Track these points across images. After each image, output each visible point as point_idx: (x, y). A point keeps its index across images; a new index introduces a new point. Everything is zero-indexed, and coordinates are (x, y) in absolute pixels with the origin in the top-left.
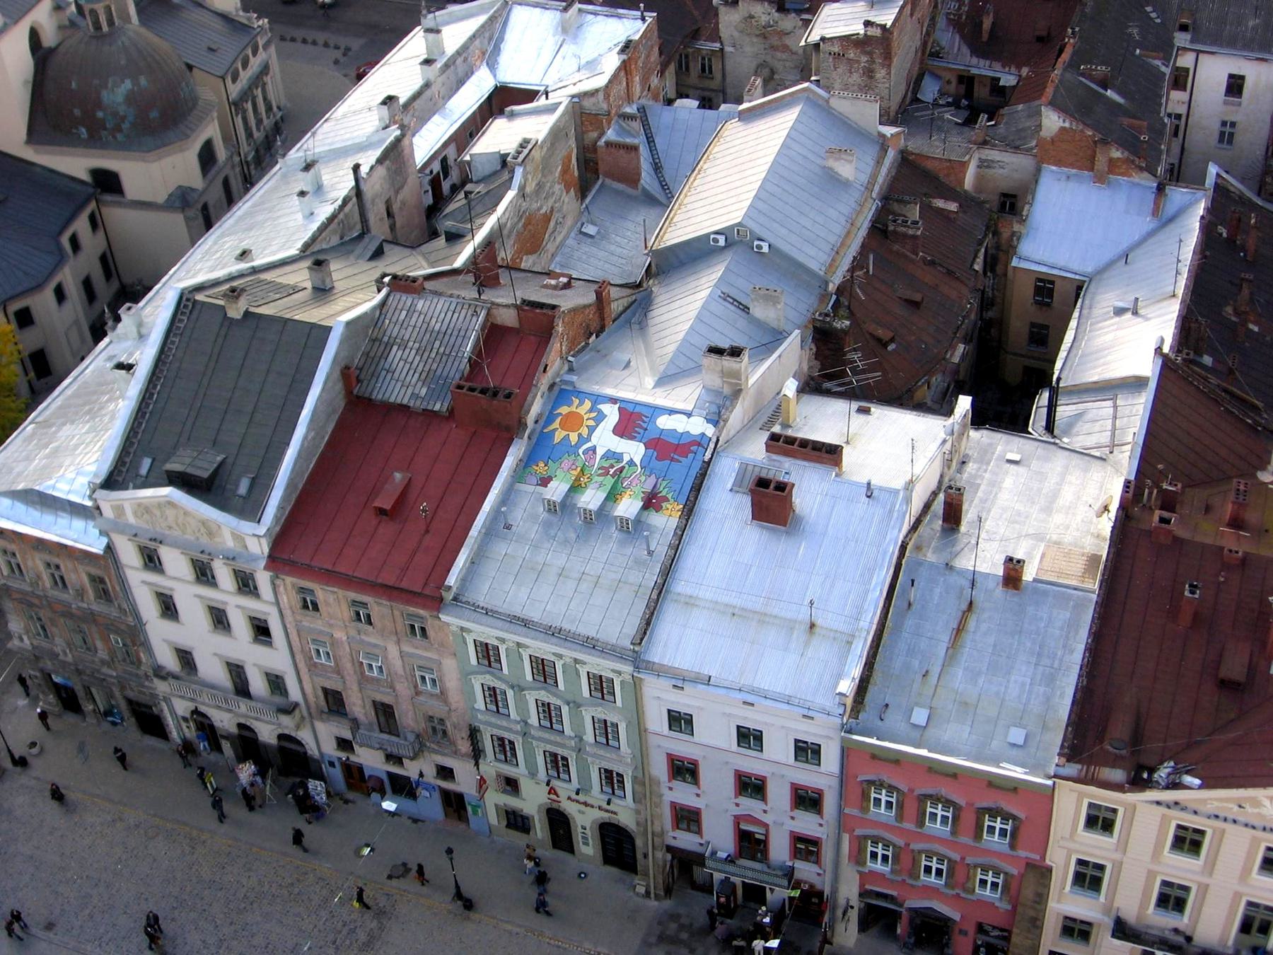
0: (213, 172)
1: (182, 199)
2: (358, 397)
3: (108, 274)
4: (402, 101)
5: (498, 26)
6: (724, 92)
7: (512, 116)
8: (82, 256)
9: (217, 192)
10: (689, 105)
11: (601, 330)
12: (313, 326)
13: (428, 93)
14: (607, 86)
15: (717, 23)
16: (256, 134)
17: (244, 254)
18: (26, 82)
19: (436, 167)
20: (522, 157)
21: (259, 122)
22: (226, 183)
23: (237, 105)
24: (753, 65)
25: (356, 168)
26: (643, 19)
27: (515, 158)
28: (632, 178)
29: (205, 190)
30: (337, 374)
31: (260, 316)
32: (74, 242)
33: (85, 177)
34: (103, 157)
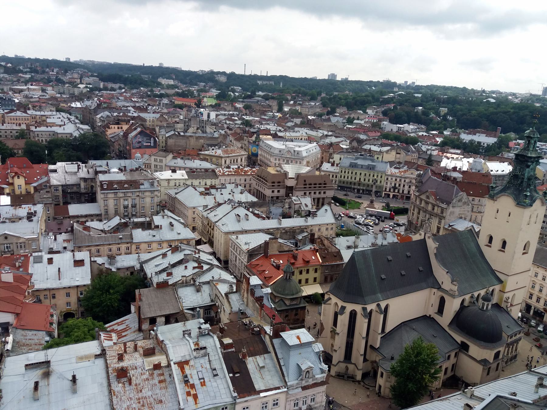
0: (496, 360)
1: (484, 362)
3: (452, 370)
9: (495, 364)
16: (509, 355)
17: (514, 394)
18: (456, 311)
21: (512, 352)
23: (508, 345)
29: (492, 363)
32: (449, 357)
33: (459, 342)
34: (467, 340)
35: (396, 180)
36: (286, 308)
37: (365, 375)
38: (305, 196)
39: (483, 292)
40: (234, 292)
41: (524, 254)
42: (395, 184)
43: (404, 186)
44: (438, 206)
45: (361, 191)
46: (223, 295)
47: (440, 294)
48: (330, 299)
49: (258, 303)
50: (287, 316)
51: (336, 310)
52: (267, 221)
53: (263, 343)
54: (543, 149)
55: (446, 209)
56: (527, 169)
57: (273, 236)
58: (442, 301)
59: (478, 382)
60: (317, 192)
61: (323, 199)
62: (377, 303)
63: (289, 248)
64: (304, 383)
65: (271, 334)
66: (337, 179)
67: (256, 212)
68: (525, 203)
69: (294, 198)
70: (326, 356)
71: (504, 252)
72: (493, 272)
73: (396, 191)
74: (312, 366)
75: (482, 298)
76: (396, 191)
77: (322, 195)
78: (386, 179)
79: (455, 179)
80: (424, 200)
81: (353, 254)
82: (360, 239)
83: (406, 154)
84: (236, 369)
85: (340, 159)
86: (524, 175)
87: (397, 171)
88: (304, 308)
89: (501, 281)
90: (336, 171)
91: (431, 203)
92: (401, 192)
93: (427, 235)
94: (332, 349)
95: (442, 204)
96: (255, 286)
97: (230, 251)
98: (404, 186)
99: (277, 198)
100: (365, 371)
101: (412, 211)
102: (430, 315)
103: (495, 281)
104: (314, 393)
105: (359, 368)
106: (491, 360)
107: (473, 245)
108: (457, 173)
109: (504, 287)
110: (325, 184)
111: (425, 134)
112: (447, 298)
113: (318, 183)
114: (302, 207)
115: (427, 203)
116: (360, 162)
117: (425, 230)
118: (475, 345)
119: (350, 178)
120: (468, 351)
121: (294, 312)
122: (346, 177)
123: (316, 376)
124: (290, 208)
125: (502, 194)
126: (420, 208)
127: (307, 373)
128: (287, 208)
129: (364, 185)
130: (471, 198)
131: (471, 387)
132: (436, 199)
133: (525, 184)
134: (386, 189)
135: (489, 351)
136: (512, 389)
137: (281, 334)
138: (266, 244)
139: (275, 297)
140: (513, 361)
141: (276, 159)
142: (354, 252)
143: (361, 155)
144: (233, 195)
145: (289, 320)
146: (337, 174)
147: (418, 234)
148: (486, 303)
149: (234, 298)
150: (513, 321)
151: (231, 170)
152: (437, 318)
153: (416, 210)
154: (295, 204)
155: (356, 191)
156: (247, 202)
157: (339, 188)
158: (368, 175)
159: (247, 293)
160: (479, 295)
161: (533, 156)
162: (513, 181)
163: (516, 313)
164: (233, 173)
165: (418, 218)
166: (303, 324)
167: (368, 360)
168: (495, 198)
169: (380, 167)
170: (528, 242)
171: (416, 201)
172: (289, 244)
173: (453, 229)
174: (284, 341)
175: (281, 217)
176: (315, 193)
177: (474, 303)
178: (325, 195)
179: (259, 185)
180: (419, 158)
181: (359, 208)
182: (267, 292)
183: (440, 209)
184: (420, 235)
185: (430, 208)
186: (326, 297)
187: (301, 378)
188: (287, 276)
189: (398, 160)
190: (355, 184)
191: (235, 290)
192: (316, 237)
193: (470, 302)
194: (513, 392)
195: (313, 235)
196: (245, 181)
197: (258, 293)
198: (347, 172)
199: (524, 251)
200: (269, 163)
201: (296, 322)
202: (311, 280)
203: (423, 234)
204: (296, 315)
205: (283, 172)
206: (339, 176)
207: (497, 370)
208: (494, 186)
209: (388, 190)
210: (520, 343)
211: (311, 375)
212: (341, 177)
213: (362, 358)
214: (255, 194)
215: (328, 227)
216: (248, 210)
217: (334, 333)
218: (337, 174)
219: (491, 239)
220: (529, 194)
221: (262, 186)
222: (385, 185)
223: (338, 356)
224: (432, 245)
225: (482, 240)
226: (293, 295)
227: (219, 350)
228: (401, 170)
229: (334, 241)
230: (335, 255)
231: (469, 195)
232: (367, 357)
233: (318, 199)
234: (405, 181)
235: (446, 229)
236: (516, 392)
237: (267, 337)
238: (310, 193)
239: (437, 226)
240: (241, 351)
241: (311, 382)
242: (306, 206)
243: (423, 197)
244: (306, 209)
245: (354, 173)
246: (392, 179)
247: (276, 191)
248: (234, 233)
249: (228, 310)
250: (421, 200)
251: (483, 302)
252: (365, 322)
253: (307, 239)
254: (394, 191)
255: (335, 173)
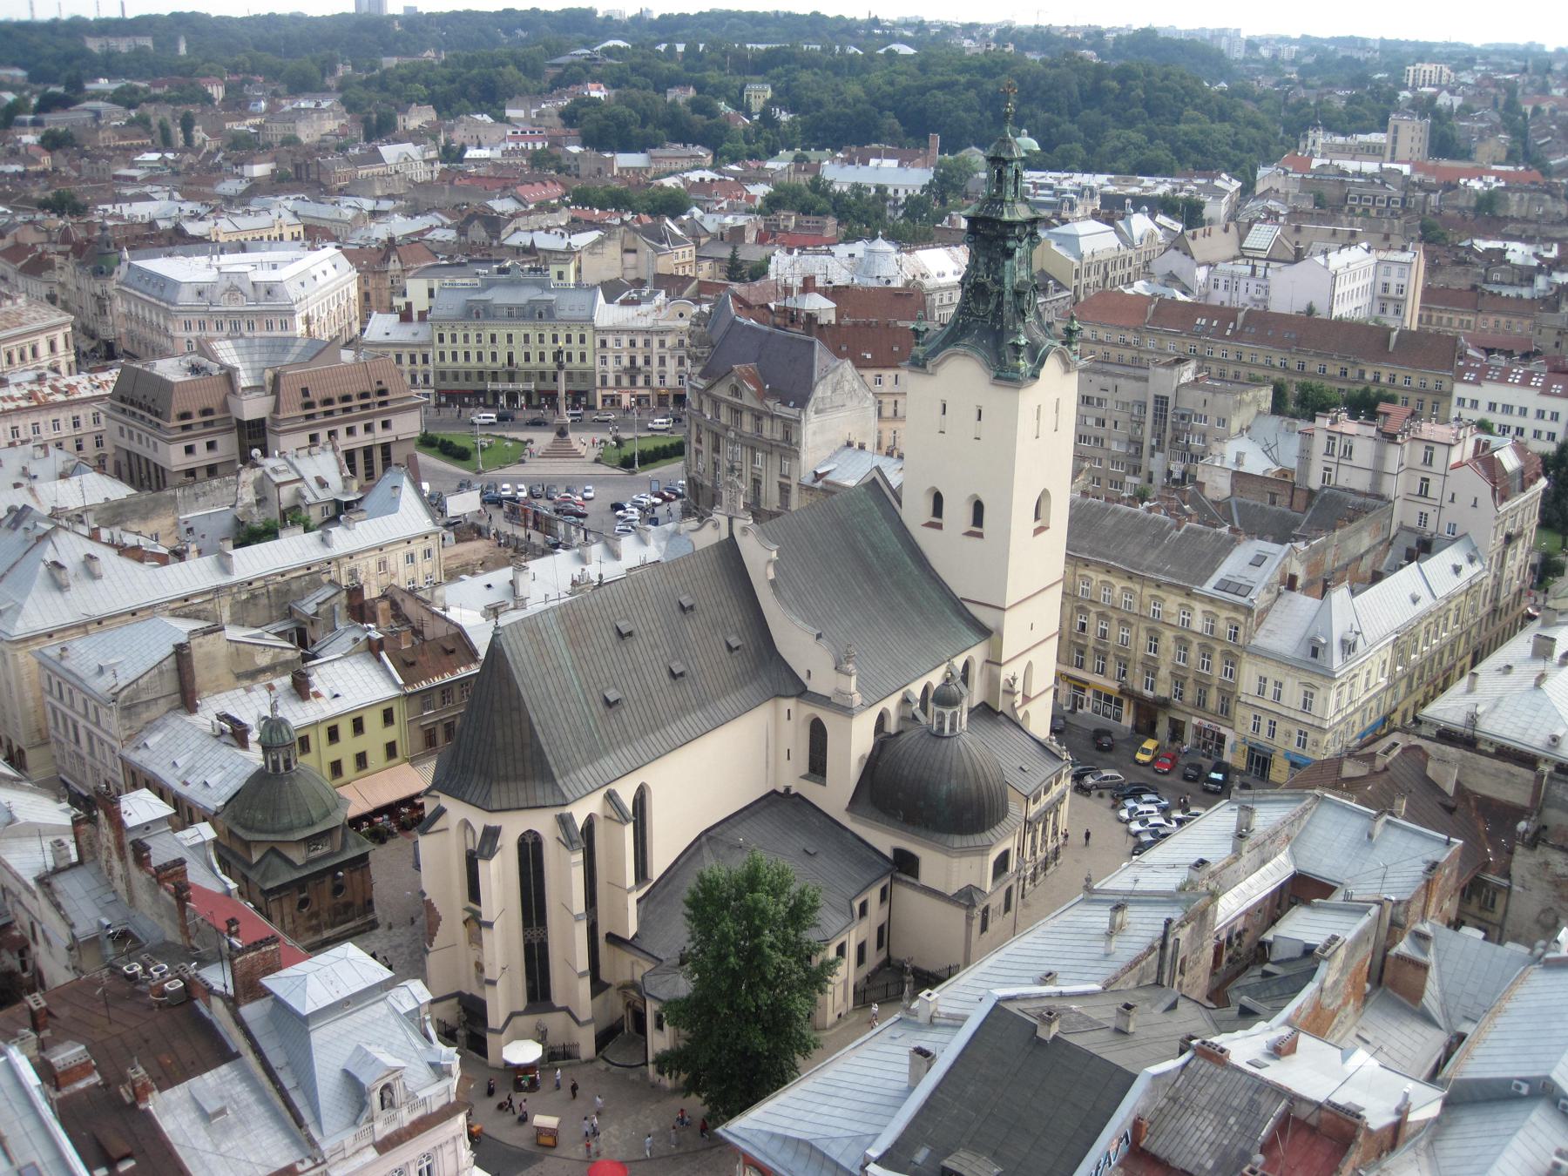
0: (1001, 880)
1: (967, 898)
2: (1142, 1150)
3: (880, 945)
4: (1214, 867)
5: (1307, 817)
6: (1501, 927)
7: (1319, 907)
8: (865, 923)
10: (1473, 934)
11: (1393, 1147)
12: (1118, 1069)
13: (1235, 866)
14: (1409, 902)
15: (1509, 862)
16: (1038, 853)
17: (1049, 977)
19: (1223, 937)
20: (1329, 951)
21: (1045, 842)
22: (1009, 892)
24: (1538, 909)
25: (1169, 922)
26: (1448, 843)
27: (1323, 951)
28: (1416, 994)
30: (1129, 1122)
31: (1068, 1044)
32: (863, 908)
33: (888, 853)
34: (911, 841)
35: (633, 343)
36: (297, 875)
37: (604, 1039)
38: (314, 450)
39: (936, 678)
40: (72, 866)
41: (1038, 531)
42: (633, 360)
43: (662, 361)
44: (772, 417)
45: (522, 400)
46: (32, 883)
47: (808, 710)
48: (440, 812)
49: (166, 889)
50: (304, 903)
51: (470, 846)
52: (175, 568)
53: (207, 1028)
54: (1064, 192)
55: (799, 422)
56: (1008, 263)
57: (206, 619)
58: (818, 733)
59: (960, 961)
60: (359, 427)
61: (386, 447)
62: (604, 791)
63: (275, 656)
64: (382, 1129)
65: (231, 991)
66: (430, 367)
67: (130, 540)
68: (1017, 370)
69: (269, 463)
70: (465, 1009)
71: (980, 535)
72: (959, 607)
73: (640, 381)
74: (402, 1064)
75: (934, 700)
76: (640, 381)
77: (380, 436)
78: (598, 344)
79: (811, 318)
80: (726, 401)
81: (495, 636)
82: (531, 570)
83: (656, 250)
84: (117, 1145)
85: (431, 293)
86: (1000, 282)
87: (630, 311)
88: (364, 858)
89: (985, 632)
90: (421, 338)
91: (751, 409)
92: (655, 381)
93: (738, 524)
94: (479, 979)
95: (784, 409)
96: (146, 827)
97: (49, 709)
98: (662, 361)
99: (212, 470)
100: (604, 1024)
101: (694, 444)
102: (788, 789)
103: (969, 636)
104: (425, 1150)
105: (582, 1019)
106: (988, 887)
107: (885, 529)
108: (816, 296)
109: (997, 649)
110: (383, 392)
111: (708, 175)
112: (830, 720)
113: (354, 390)
114: (306, 492)
115: (737, 411)
116: (500, 297)
117: (730, 507)
118: (933, 848)
119: (474, 357)
120: (916, 875)
121: (328, 879)
122: (461, 357)
123: (421, 1095)
124: (261, 502)
125: (950, 350)
126: (716, 429)
127: (387, 1095)
128: (251, 505)
129: (528, 376)
130: (870, 375)
131: (928, 991)
132: (761, 395)
133: (1008, 311)
134: (604, 380)
135: (976, 860)
136: (1045, 961)
137: (269, 982)
138: (181, 653)
139: (247, 845)
140: (1052, 868)
141: (188, 326)
142: (497, 628)
143: (502, 271)
144: (32, 490)
145: (315, 915)
146: (425, 350)
147: (709, 525)
148: (948, 712)
149: (72, 888)
150: (1033, 745)
151: (16, 393)
152: (811, 791)
153: (707, 439)
154: (279, 485)
155: (503, 400)
156: (86, 510)
157: (443, 399)
158: (534, 338)
159: (122, 858)
160: (926, 690)
161: (1018, 218)
162: (972, 304)
163: (1039, 720)
164: (23, 404)
165: (716, 464)
166: (370, 917)
167: (608, 986)
168: (929, 367)
169: (568, 305)
170: (1045, 494)
171: (701, 410)
172: (270, 639)
173: (829, 487)
174: (280, 1005)
175: (230, 544)
176: (350, 431)
177: (915, 718)
178: (387, 433)
179: (131, 433)
180: (699, 258)
181: (523, 462)
182: (199, 840)
183: (778, 425)
184: (716, 526)
185: (747, 425)
186: (429, 808)
187: (365, 1115)
188: (275, 763)
189: (632, 275)
190: (495, 376)
191: (74, 858)
192: (371, 592)
193: (902, 719)
194: (1047, 969)
195: (355, 592)
196: (76, 424)
197: (162, 850)
198: (460, 338)
199: (1038, 524)
200: (166, 342)
201: (339, 918)
202: (376, 757)
203: (724, 521)
204: (338, 889)
205: (216, 373)
206: (433, 354)
207: (1007, 908)
208: (922, 329)
209: (611, 382)
210: (1064, 808)
211: (399, 1095)
212: (442, 355)
213: (587, 981)
214: (125, 470)
215: (413, 547)
216: (94, 536)
217: (476, 923)
218: (425, 350)
219: (938, 500)
220: (1023, 342)
221: (144, 435)
222: (599, 367)
223: (505, 996)
224: (759, 556)
225: (915, 512)
226: (311, 824)
227: (37, 1095)
228: (644, 308)
229: (442, 598)
230: (450, 647)
231: (860, 364)
232: (604, 975)
233: (368, 451)
234: (662, 344)
235: (809, 489)
236: (1052, 969)
237: (218, 1004)
238: (331, 433)
239: (780, 484)
240: (123, 1079)
241: (406, 1117)
242: (323, 484)
243: (722, 391)
244: (323, 495)
245: (486, 338)
246: (618, 342)
247: (200, 445)
248: (50, 635)
249: (60, 936)
250: (716, 402)
251: (938, 709)
252: (575, 864)
253: (337, 608)
254: (633, 382)
255: (419, 346)
